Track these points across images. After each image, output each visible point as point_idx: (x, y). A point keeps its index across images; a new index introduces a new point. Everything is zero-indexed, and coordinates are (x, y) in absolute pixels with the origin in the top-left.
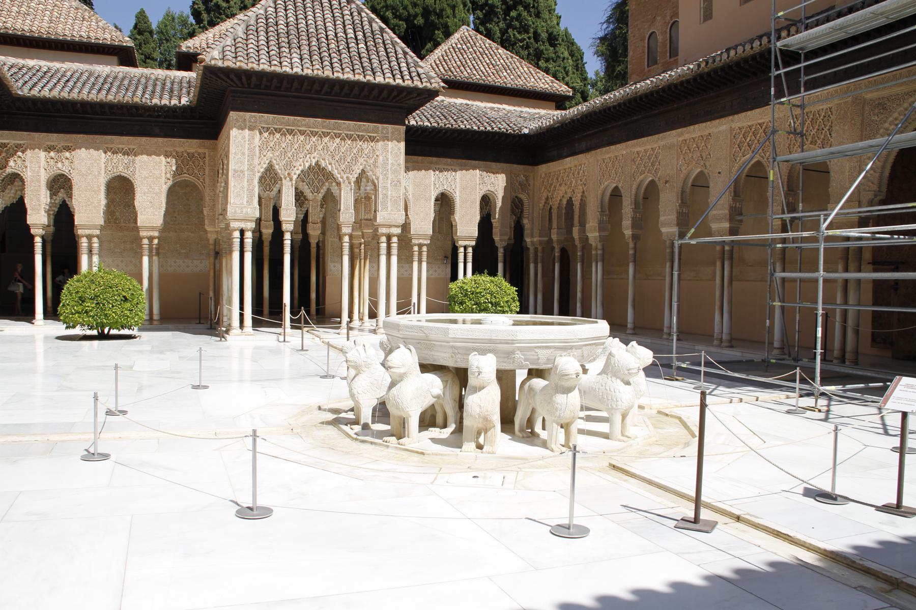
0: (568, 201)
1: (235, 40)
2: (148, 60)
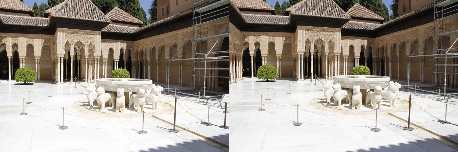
0: (142, 50)
1: (59, 10)
2: (37, 15)
